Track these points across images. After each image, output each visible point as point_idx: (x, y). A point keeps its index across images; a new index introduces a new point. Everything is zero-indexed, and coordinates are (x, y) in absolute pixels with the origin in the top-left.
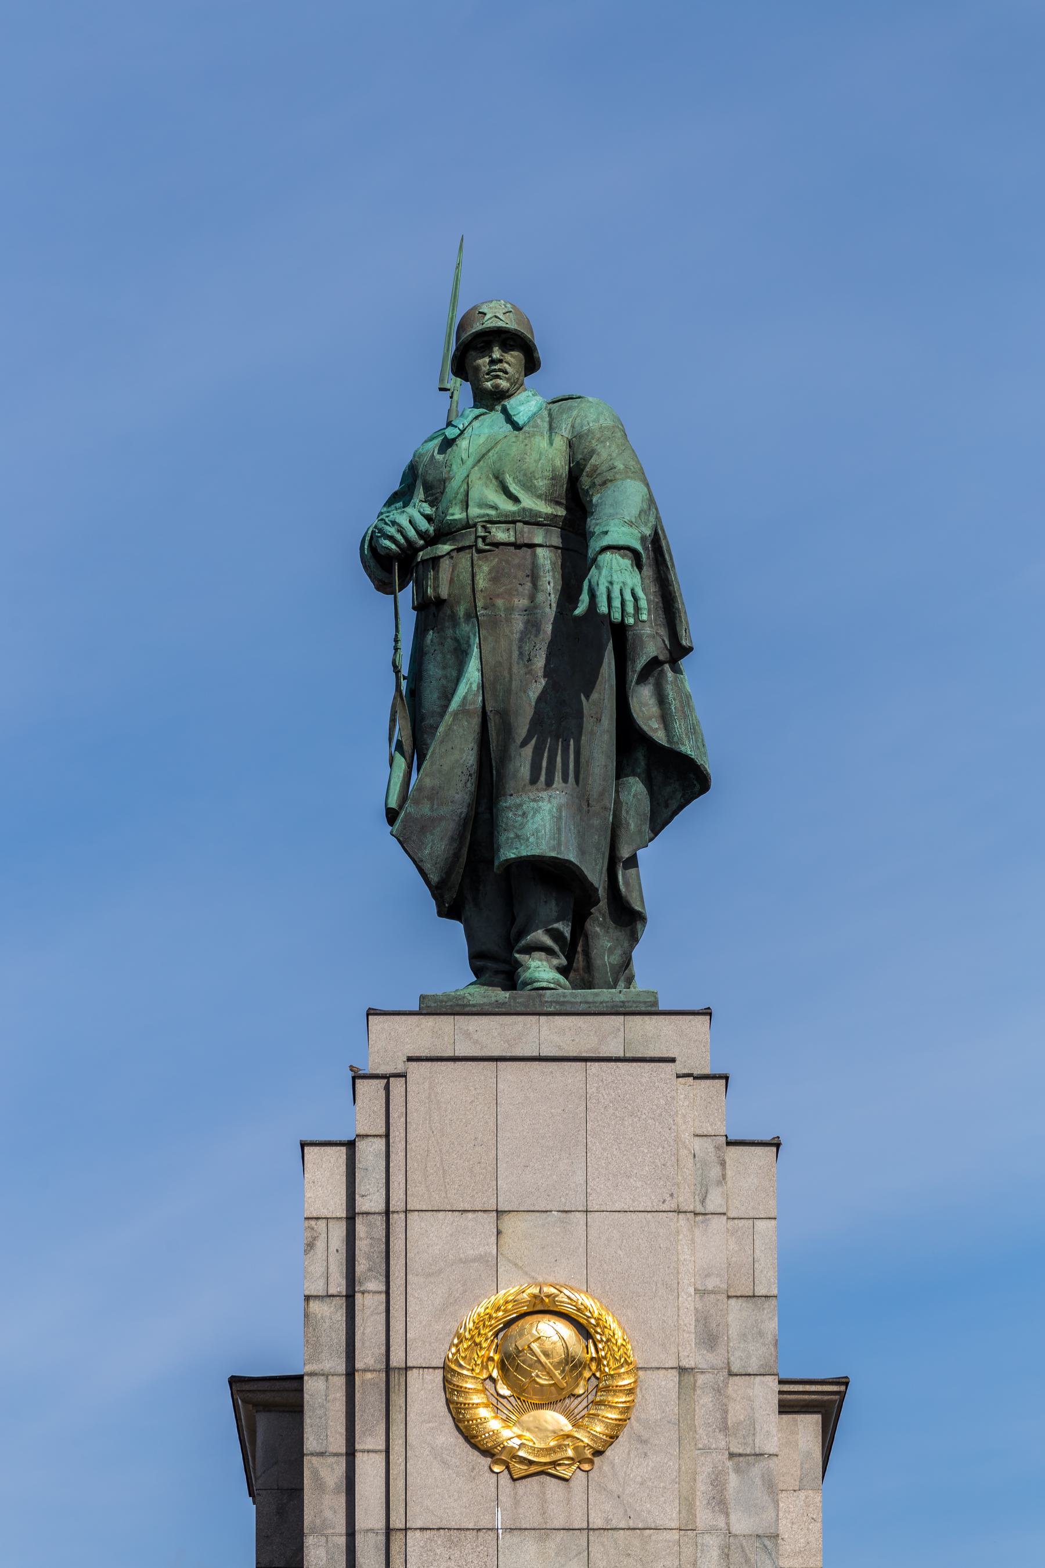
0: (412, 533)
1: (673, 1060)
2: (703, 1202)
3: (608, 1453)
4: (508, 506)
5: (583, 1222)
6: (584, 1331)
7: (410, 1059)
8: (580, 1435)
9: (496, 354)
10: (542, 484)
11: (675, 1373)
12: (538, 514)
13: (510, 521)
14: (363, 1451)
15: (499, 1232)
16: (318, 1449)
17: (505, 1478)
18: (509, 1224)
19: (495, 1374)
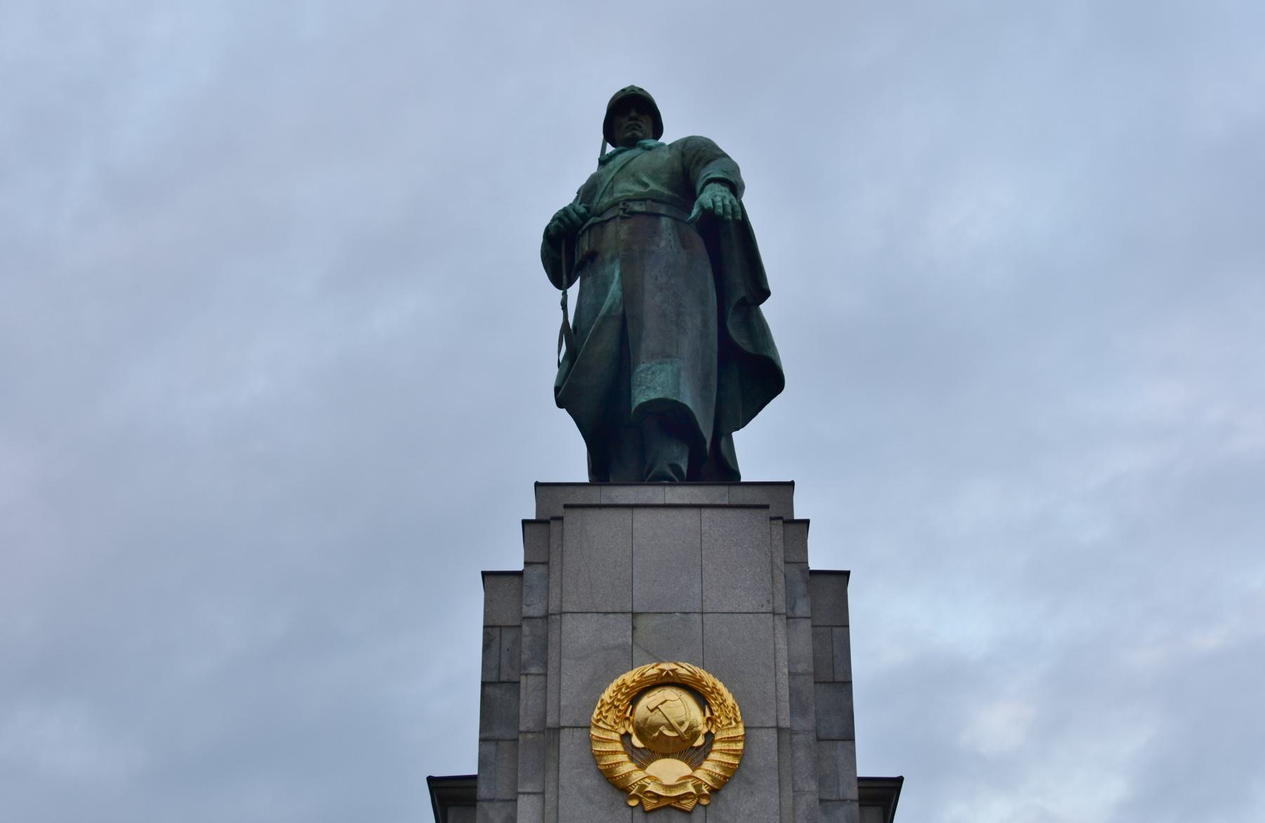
0: (574, 216)
1: (766, 507)
2: (793, 609)
3: (722, 792)
4: (638, 189)
5: (699, 621)
6: (701, 696)
7: (566, 506)
8: (699, 774)
9: (633, 114)
10: (664, 176)
11: (774, 731)
12: (662, 194)
13: (641, 199)
14: (524, 793)
15: (634, 628)
16: (488, 796)
17: (638, 814)
18: (642, 622)
19: (631, 730)
